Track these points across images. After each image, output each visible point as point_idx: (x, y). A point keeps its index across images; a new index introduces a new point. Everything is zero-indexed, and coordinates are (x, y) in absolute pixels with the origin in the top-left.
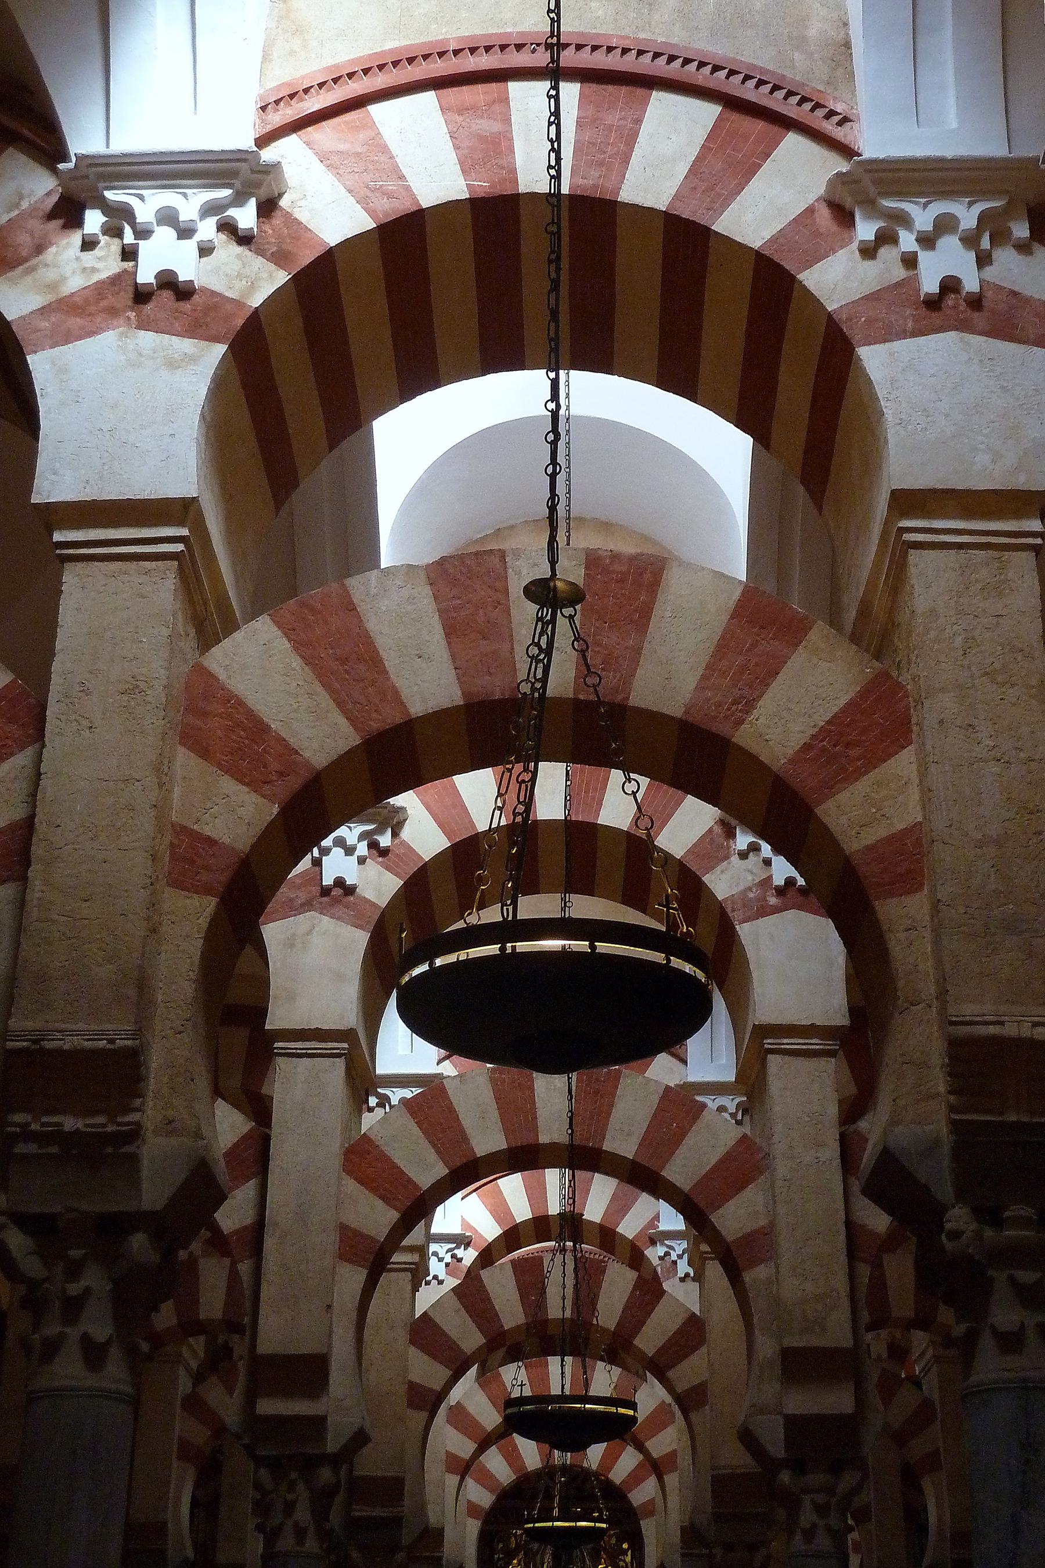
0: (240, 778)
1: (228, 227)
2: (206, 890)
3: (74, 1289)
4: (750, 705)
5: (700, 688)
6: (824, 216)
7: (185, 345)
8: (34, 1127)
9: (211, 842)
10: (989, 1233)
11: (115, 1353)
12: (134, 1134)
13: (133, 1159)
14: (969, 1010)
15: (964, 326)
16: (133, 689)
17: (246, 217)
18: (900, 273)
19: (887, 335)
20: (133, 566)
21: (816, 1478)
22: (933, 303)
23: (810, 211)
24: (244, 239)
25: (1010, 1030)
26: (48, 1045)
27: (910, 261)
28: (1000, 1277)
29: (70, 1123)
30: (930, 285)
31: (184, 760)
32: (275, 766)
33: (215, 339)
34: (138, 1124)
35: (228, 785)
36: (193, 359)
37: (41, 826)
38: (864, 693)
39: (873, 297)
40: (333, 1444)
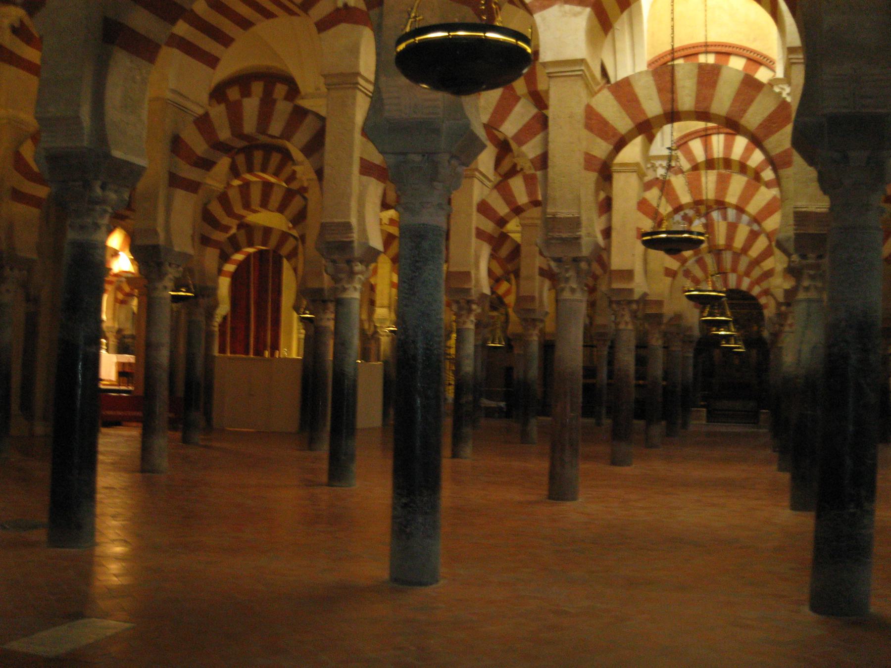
0: (602, 137)
2: (594, 170)
3: (567, 275)
7: (578, 9)
9: (595, 157)
12: (579, 238)
13: (579, 244)
14: (799, 204)
16: (571, 116)
20: (568, 78)
25: (809, 210)
26: (557, 216)
29: (564, 235)
31: (585, 133)
33: (586, 6)
34: (579, 235)
35: (599, 140)
36: (580, 13)
37: (550, 156)
38: (778, 108)
40: (636, 296)
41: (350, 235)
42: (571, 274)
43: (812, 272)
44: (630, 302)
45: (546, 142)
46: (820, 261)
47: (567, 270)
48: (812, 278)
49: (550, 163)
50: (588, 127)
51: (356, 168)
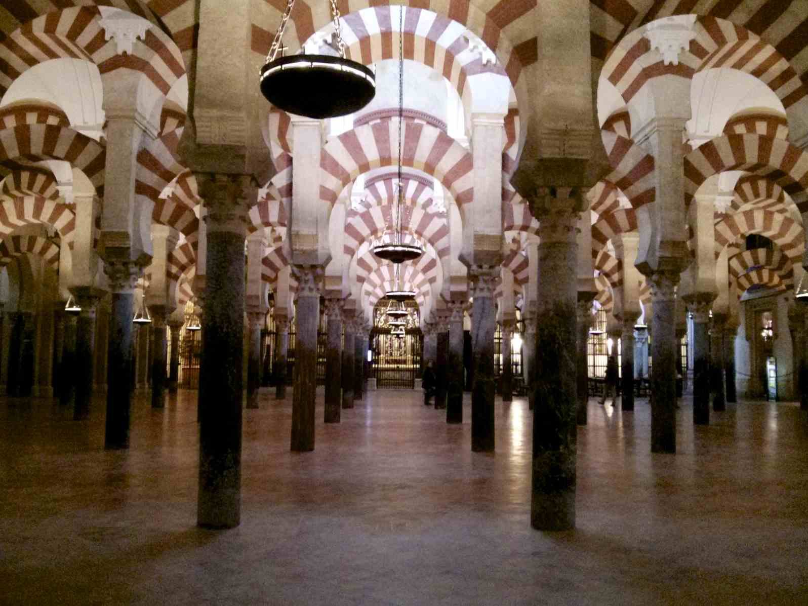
1: (326, 42)
4: (439, 160)
5: (429, 156)
6: (462, 40)
8: (297, 248)
10: (480, 270)
11: (315, 290)
14: (478, 229)
15: (491, 71)
17: (330, 40)
18: (478, 56)
19: (474, 73)
21: (458, 305)
22: (485, 65)
23: (459, 39)
24: (329, 45)
27: (481, 54)
28: (481, 278)
30: (484, 62)
31: (321, 170)
32: (340, 172)
39: (472, 63)
41: (127, 242)
42: (310, 277)
43: (486, 278)
44: (338, 300)
45: (291, 176)
46: (491, 271)
47: (306, 275)
48: (486, 281)
49: (294, 191)
50: (323, 165)
51: (132, 186)
